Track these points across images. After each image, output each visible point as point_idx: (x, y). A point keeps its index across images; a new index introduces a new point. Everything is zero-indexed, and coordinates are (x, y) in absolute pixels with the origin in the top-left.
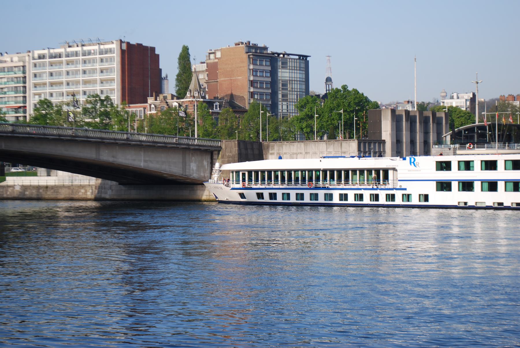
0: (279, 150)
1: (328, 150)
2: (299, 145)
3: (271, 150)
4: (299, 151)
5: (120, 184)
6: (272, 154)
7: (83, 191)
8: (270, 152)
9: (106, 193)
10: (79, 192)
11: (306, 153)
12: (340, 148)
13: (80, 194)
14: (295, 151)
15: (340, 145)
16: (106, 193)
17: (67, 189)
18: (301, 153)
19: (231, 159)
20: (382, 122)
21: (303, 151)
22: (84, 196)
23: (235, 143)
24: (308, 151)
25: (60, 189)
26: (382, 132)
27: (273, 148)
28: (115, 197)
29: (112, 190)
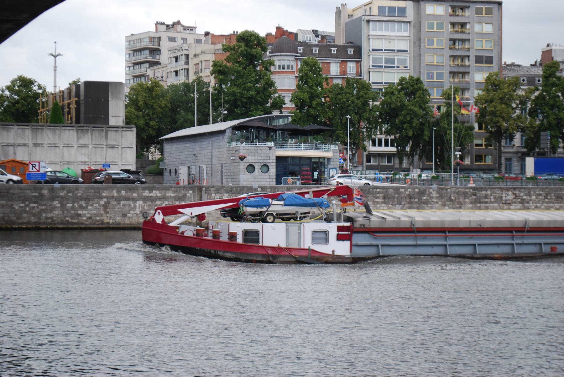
1: (81, 142)
2: (20, 131)
4: (20, 141)
11: (36, 145)
12: (90, 140)
14: (11, 141)
15: (104, 134)
18: (24, 145)
20: (110, 102)
21: (30, 143)
24: (39, 142)
26: (110, 118)
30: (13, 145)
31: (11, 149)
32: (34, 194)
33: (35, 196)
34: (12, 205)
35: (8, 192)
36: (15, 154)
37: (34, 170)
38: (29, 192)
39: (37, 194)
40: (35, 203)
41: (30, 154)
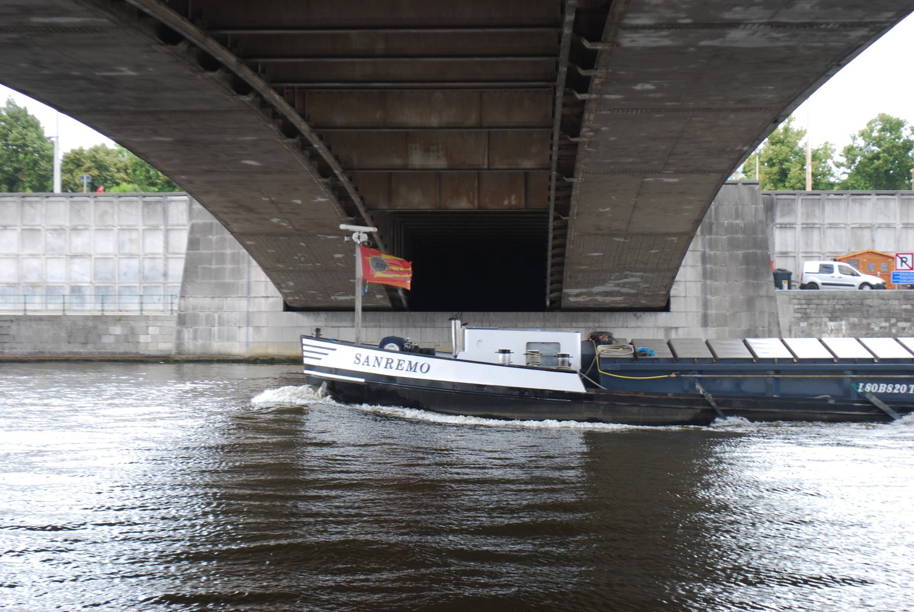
0: (808, 215)
2: (881, 203)
3: (783, 215)
4: (882, 220)
5: (288, 308)
6: (783, 227)
7: (117, 330)
8: (779, 220)
9: (231, 338)
10: (99, 336)
13: (107, 340)
14: (867, 220)
16: (231, 338)
17: (44, 326)
18: (888, 226)
19: (740, 236)
21: (898, 222)
22: (123, 349)
23: (753, 190)
25: (14, 327)
27: (790, 211)
28: (272, 351)
29: (258, 328)
30: (870, 227)
31: (867, 233)
32: (904, 307)
33: (906, 310)
34: (869, 324)
35: (862, 304)
36: (873, 241)
37: (905, 267)
38: (896, 302)
39: (909, 307)
40: (906, 320)
41: (898, 241)
